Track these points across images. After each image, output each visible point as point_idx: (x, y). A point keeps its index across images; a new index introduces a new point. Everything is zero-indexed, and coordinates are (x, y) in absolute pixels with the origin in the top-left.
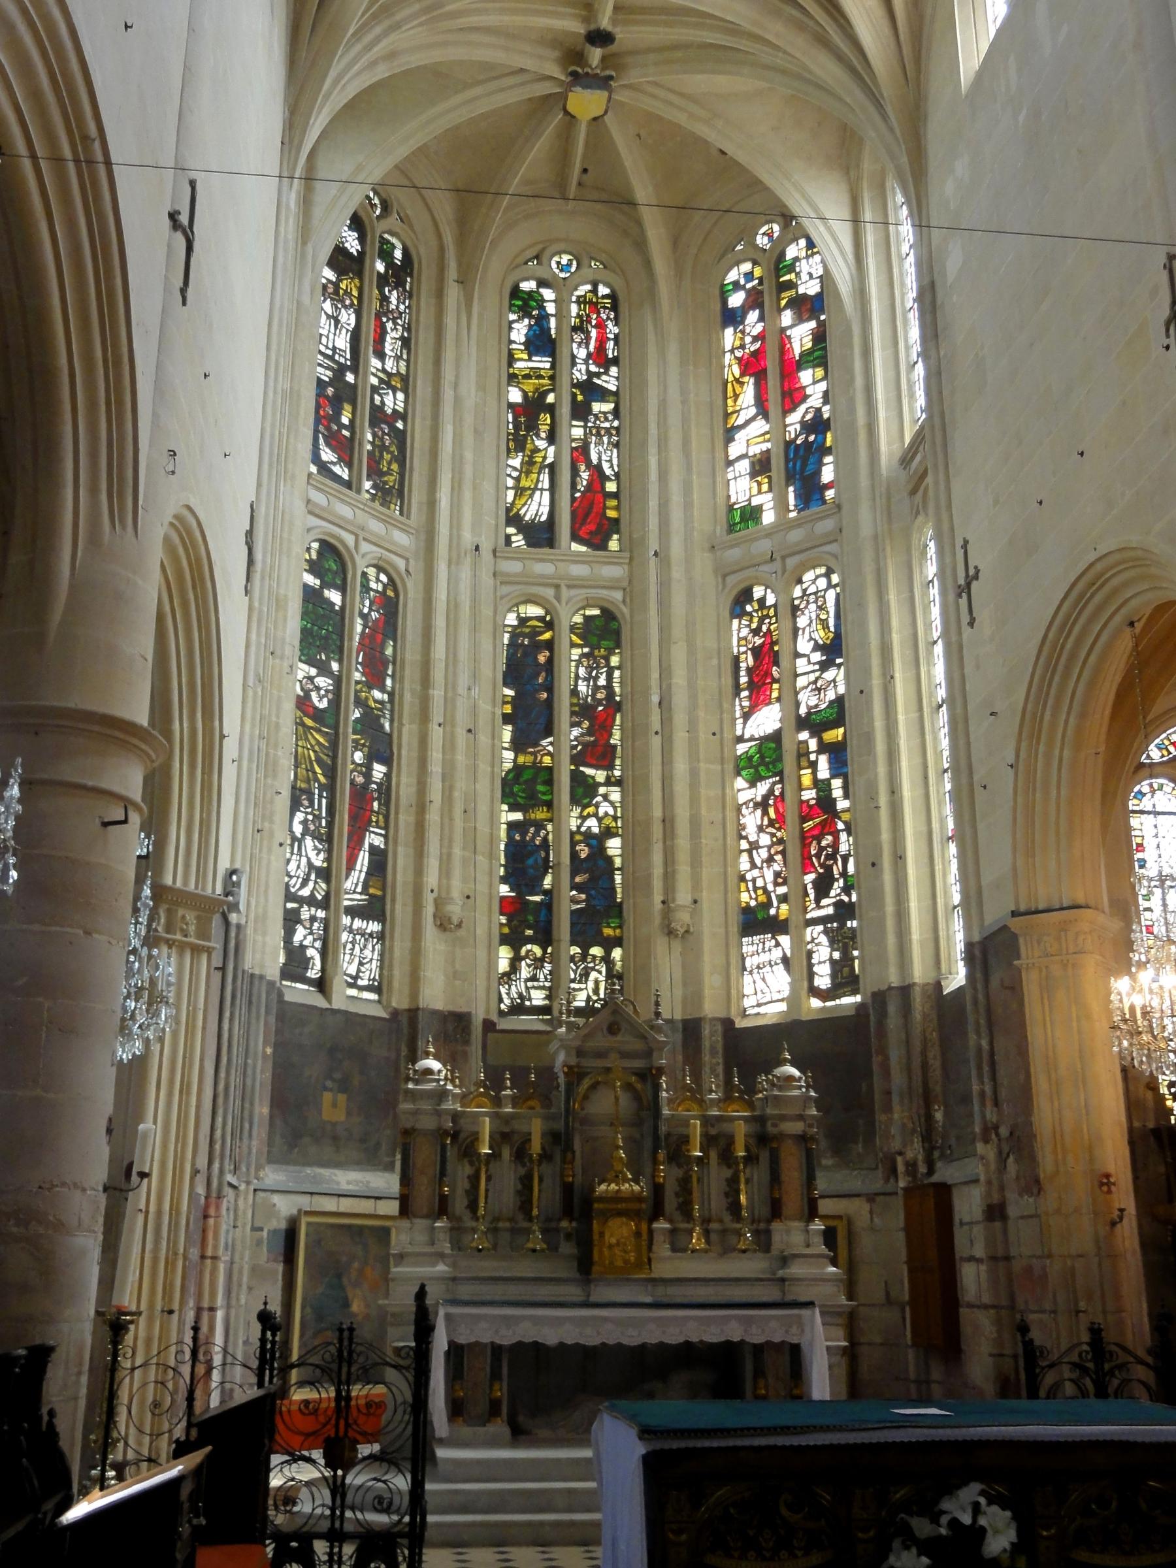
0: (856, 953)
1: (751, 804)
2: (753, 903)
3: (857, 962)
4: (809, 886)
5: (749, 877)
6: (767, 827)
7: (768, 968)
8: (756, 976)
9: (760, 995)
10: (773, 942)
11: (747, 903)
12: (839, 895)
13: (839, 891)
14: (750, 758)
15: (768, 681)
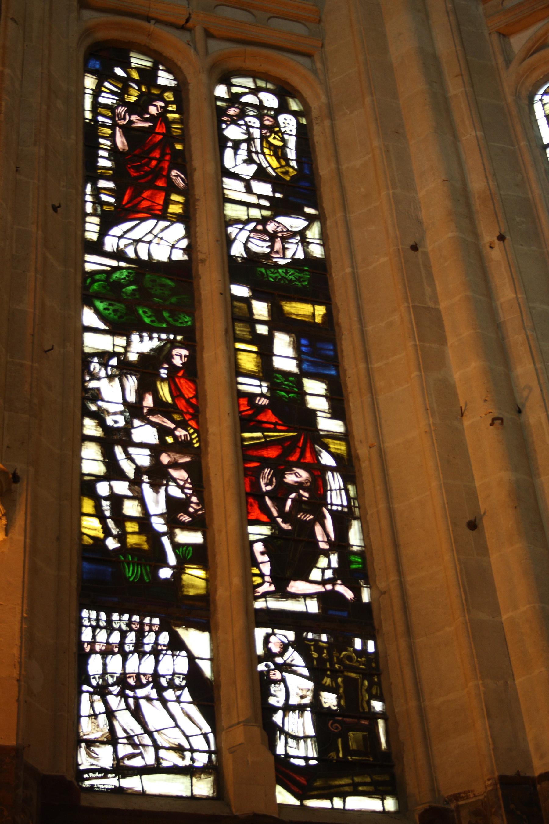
0: (378, 706)
1: (114, 362)
2: (112, 544)
3: (381, 724)
4: (259, 547)
5: (103, 489)
6: (152, 411)
7: (150, 691)
8: (114, 701)
9: (124, 750)
10: (164, 638)
11: (99, 543)
12: (332, 581)
13: (329, 574)
14: (118, 286)
15: (160, 183)
